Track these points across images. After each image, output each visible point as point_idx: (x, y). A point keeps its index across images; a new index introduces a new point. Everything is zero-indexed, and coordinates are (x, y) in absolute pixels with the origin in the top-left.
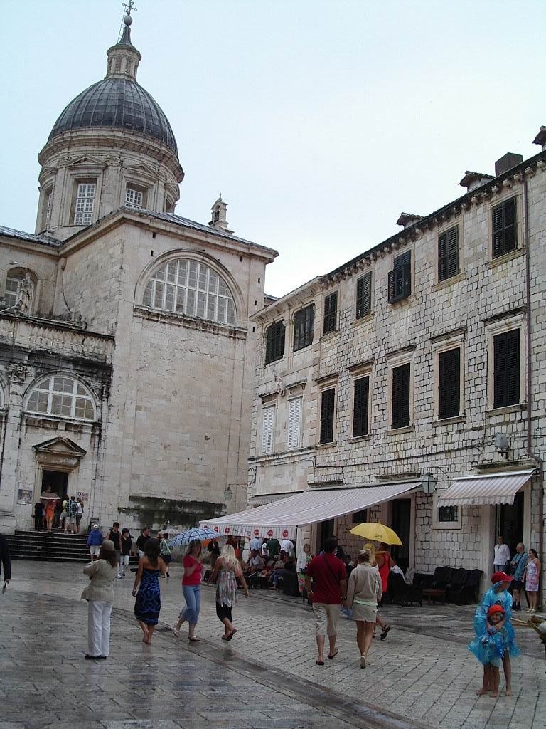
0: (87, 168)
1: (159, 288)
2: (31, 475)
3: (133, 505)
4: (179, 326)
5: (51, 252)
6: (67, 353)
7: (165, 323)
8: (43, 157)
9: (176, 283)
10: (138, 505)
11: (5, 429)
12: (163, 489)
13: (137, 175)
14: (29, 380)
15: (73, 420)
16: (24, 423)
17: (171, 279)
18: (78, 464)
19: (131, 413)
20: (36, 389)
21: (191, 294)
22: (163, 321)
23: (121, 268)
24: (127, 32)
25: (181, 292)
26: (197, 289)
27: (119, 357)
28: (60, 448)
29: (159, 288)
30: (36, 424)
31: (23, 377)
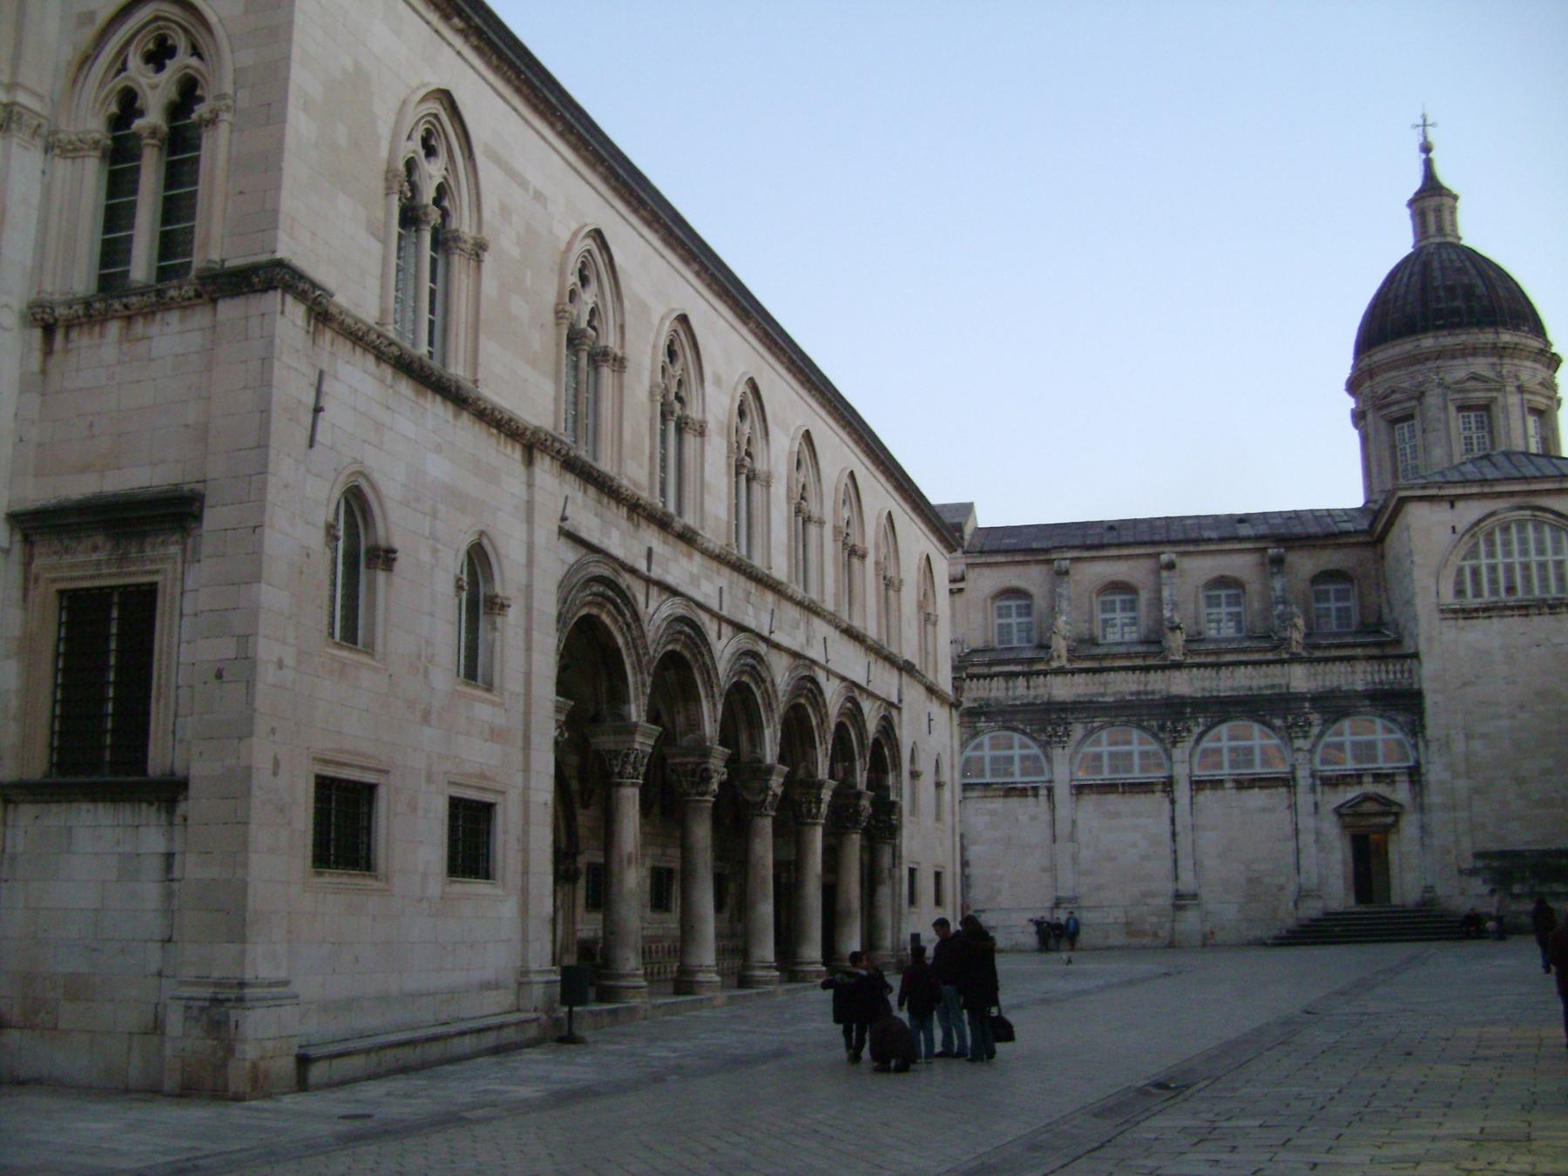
0: (1397, 402)
1: (1475, 572)
2: (1338, 844)
3: (1480, 864)
4: (1512, 616)
5: (1361, 539)
6: (1360, 687)
7: (1490, 617)
8: (1353, 387)
9: (1500, 559)
10: (1487, 862)
11: (1295, 794)
12: (1521, 837)
13: (1468, 391)
14: (1315, 730)
15: (1380, 768)
16: (1318, 782)
17: (1491, 554)
18: (1396, 822)
19: (1459, 746)
20: (1328, 739)
21: (1526, 567)
22: (1486, 614)
23: (1412, 562)
24: (1428, 164)
25: (1509, 569)
26: (1534, 558)
27: (1430, 677)
28: (1369, 807)
29: (1475, 572)
30: (1334, 782)
31: (1307, 729)
